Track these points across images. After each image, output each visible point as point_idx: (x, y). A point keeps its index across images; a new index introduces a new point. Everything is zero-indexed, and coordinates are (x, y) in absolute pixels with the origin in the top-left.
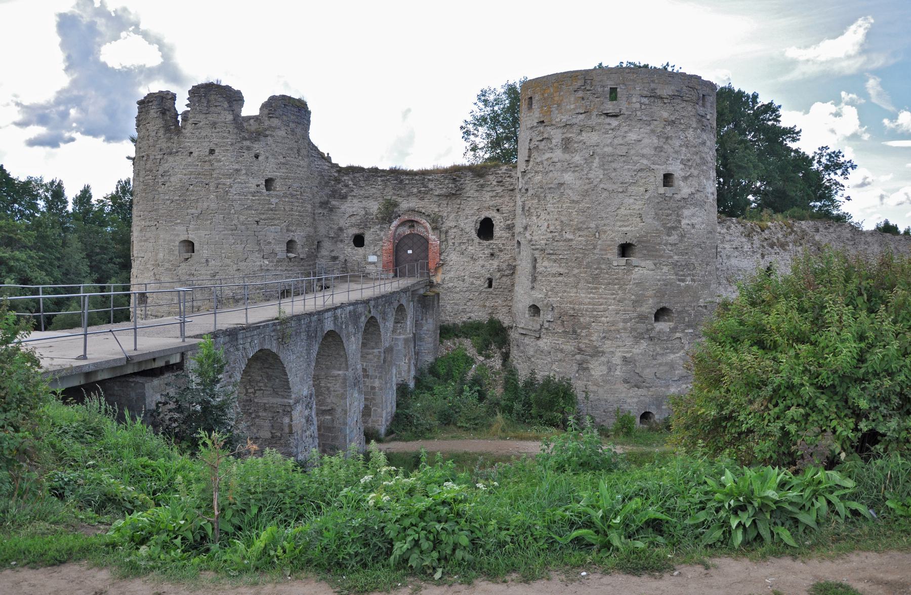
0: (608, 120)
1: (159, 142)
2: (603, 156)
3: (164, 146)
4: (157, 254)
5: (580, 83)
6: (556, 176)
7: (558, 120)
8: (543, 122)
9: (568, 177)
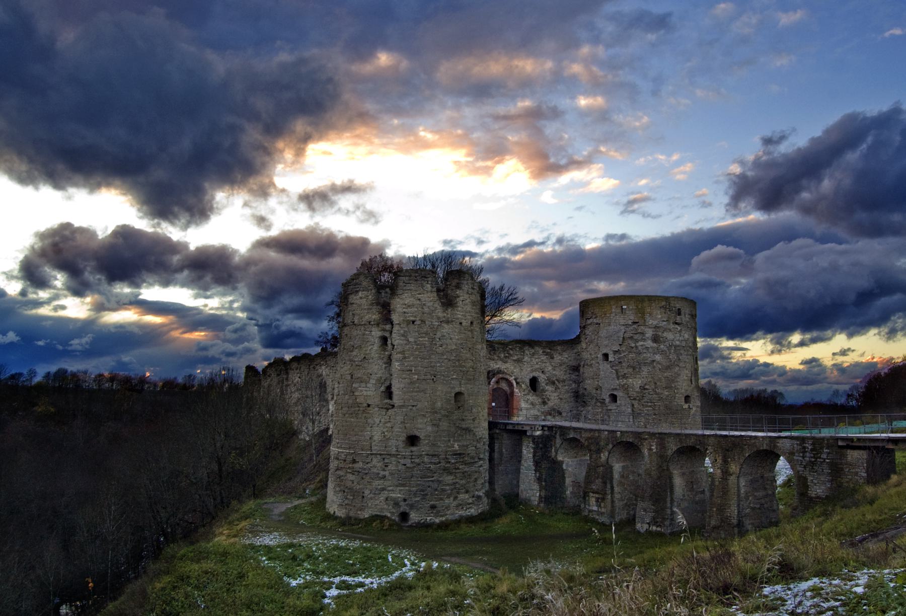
0: (676, 326)
2: (676, 346)
3: (440, 315)
4: (434, 403)
5: (664, 303)
6: (648, 356)
9: (658, 357)
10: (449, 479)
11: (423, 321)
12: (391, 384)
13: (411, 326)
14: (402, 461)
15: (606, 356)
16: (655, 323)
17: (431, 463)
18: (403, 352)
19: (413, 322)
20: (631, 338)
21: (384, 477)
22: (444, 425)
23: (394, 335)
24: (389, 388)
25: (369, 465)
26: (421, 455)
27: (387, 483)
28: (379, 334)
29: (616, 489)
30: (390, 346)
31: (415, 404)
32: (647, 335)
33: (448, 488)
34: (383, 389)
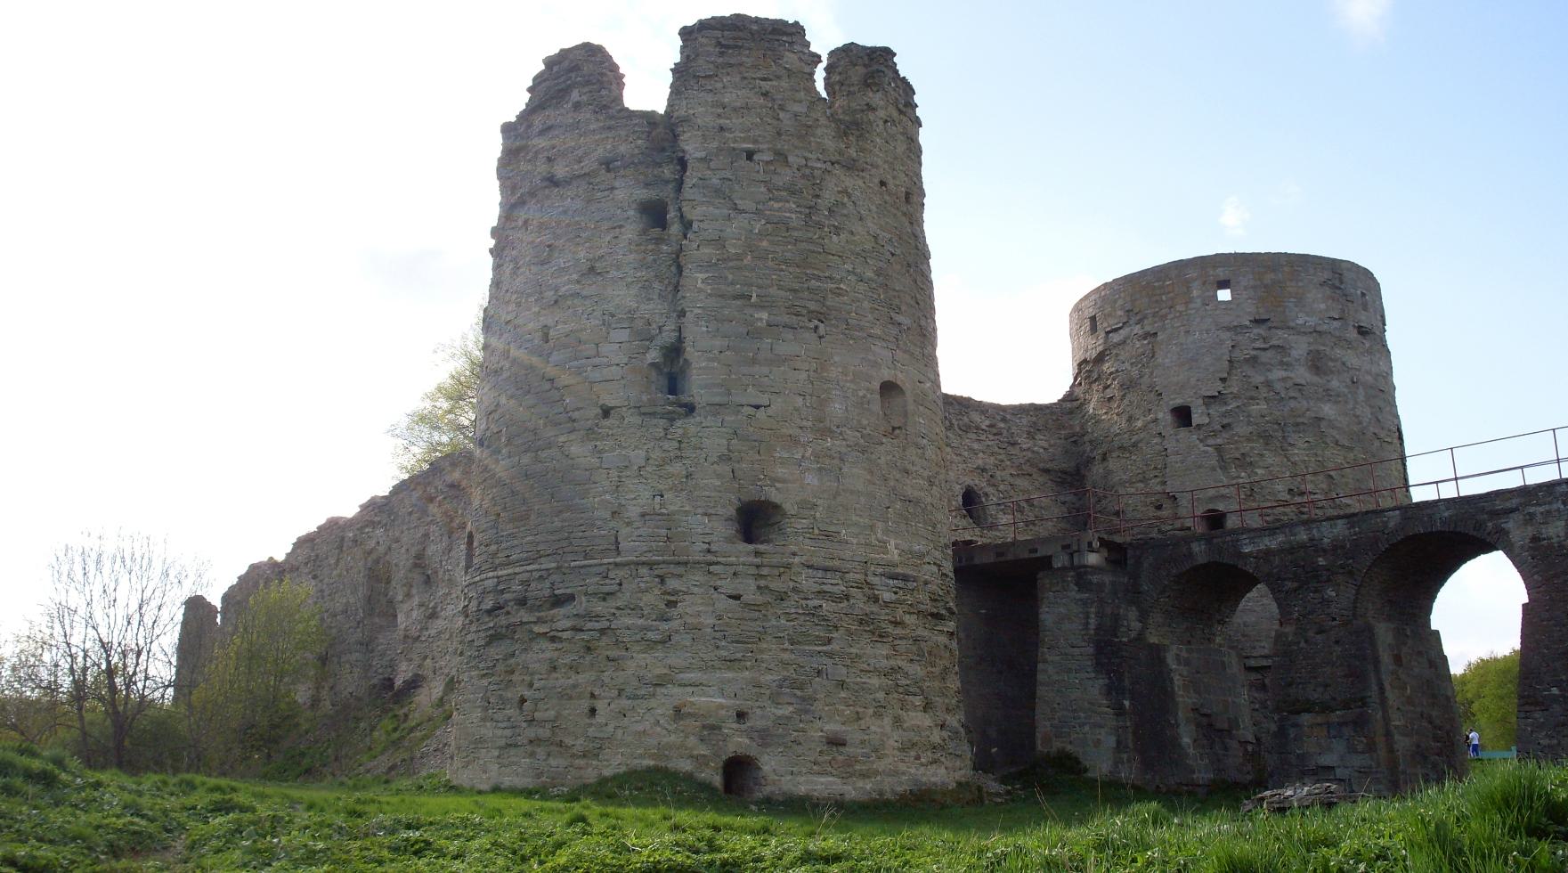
1: (819, 132)
5: (1327, 275)
7: (1300, 322)
8: (1265, 321)
10: (879, 654)
11: (781, 157)
12: (680, 339)
13: (743, 162)
14: (728, 586)
15: (1183, 415)
16: (1312, 321)
17: (821, 594)
18: (719, 242)
19: (750, 155)
20: (1253, 361)
21: (666, 640)
22: (856, 475)
23: (688, 192)
24: (674, 352)
25: (612, 603)
26: (788, 566)
27: (676, 659)
28: (642, 194)
29: (1391, 695)
30: (675, 229)
31: (764, 400)
32: (1294, 353)
33: (875, 681)
34: (653, 355)
